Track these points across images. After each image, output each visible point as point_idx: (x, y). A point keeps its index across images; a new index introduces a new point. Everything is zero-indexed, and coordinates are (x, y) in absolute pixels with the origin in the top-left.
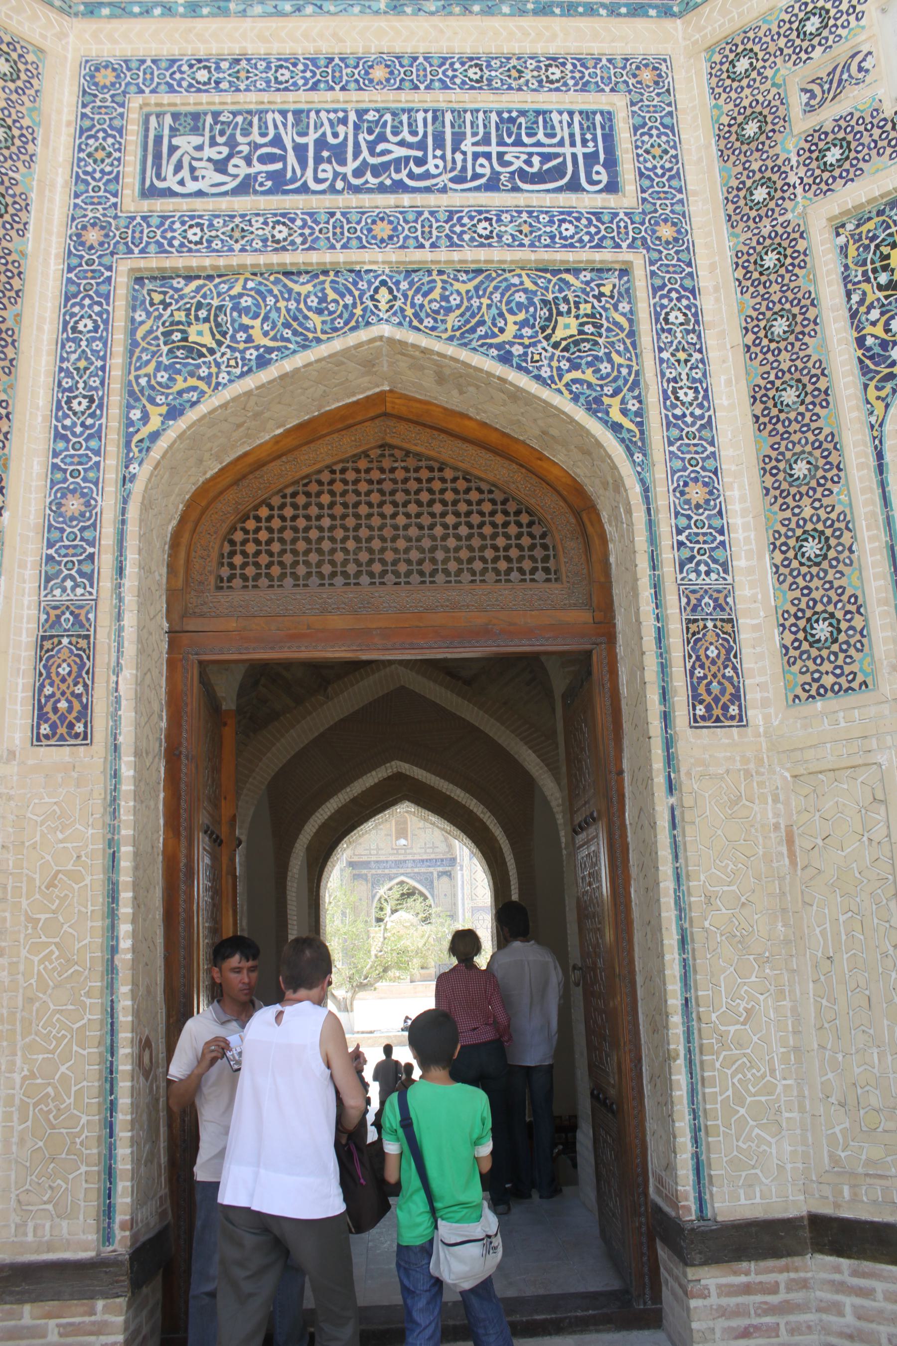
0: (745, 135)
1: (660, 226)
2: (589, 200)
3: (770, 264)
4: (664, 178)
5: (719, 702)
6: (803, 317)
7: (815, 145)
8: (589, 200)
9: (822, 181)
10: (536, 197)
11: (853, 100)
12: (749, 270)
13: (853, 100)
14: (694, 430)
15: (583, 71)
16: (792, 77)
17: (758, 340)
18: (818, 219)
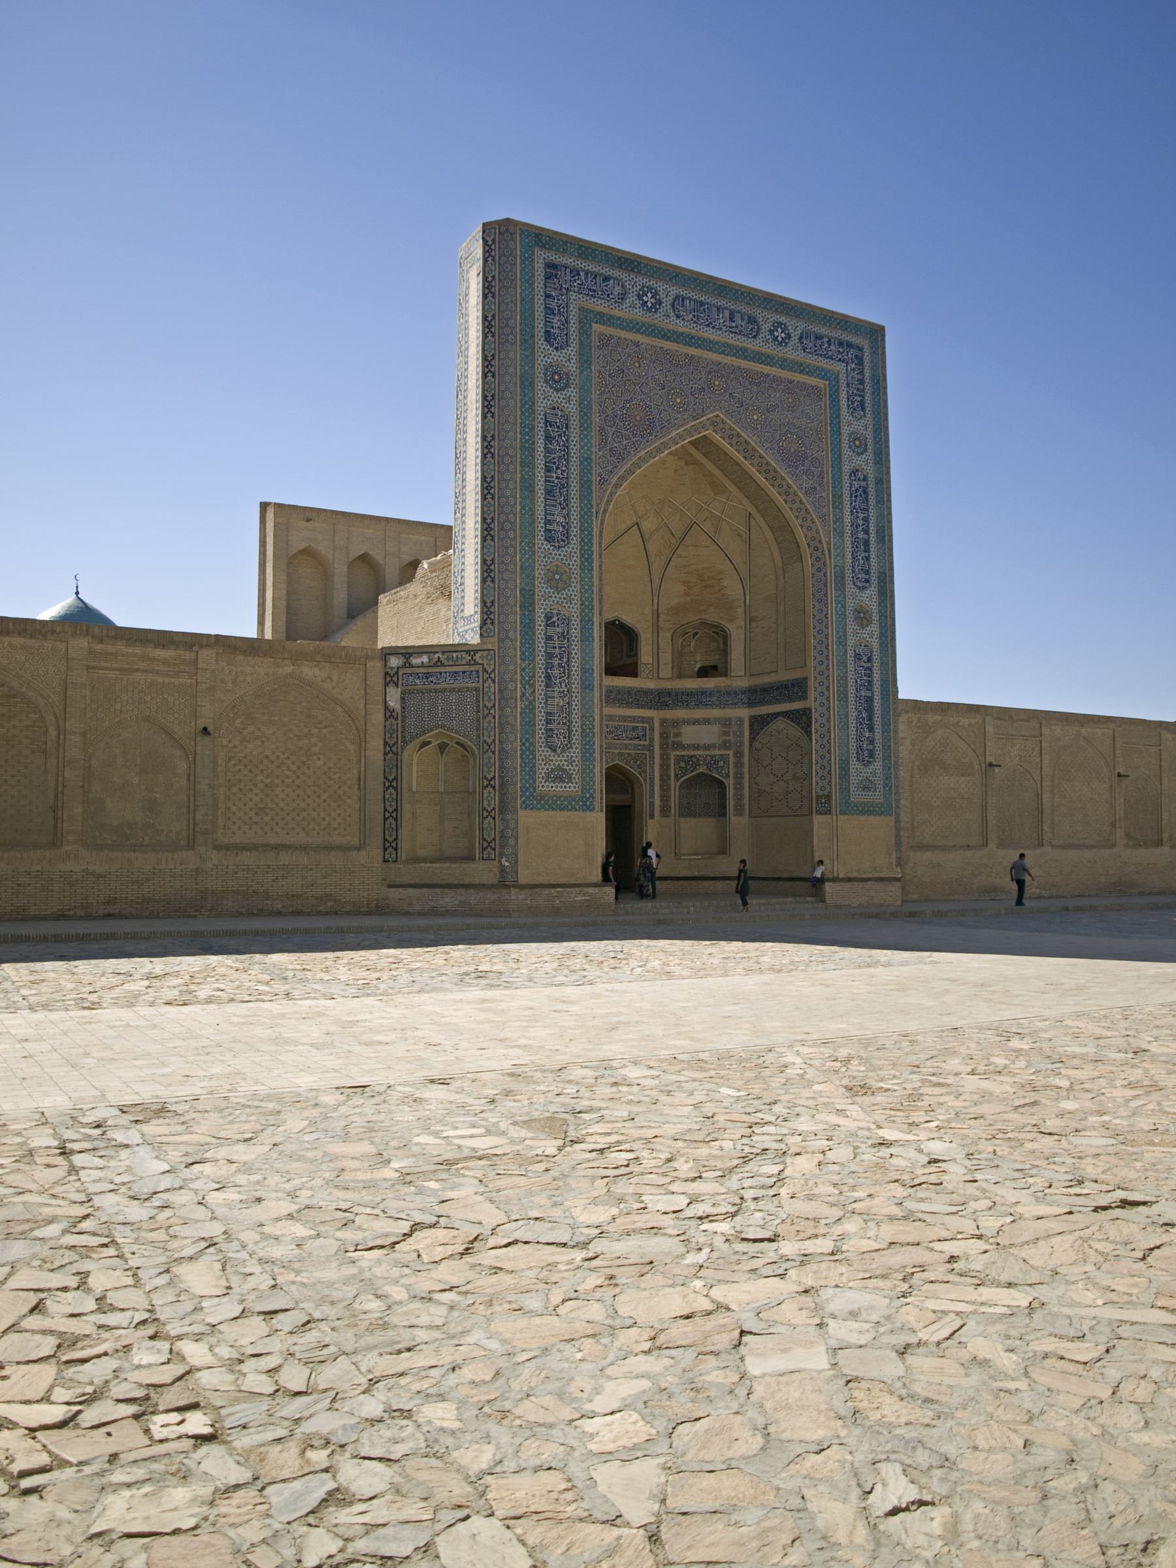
0: (664, 736)
1: (650, 748)
2: (642, 743)
3: (665, 758)
4: (652, 740)
5: (652, 816)
6: (668, 768)
7: (674, 743)
8: (642, 743)
9: (675, 749)
10: (636, 742)
11: (679, 739)
12: (662, 756)
13: (679, 739)
14: (652, 779)
15: (644, 720)
16: (673, 731)
17: (662, 766)
18: (673, 754)
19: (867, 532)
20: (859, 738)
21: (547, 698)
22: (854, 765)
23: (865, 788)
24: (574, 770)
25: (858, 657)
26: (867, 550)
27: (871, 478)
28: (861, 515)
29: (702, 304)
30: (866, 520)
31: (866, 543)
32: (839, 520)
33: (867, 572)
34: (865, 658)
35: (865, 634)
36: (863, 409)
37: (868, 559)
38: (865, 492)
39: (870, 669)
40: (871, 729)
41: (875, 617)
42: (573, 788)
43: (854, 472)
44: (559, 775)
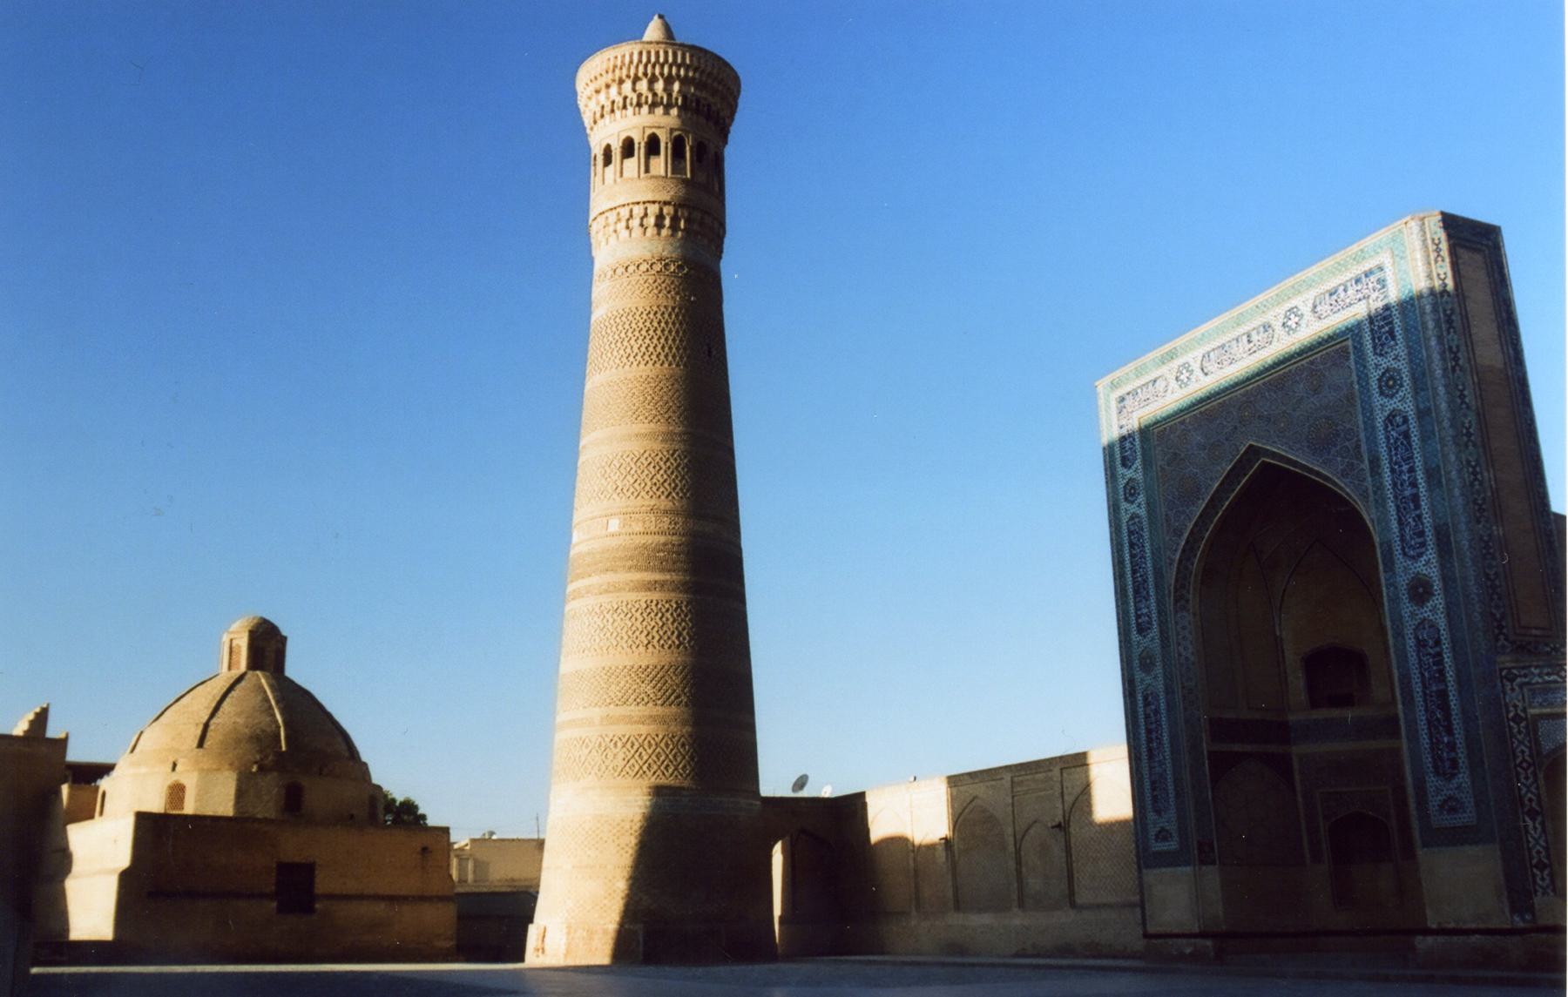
19: (1414, 485)
20: (1435, 745)
21: (1151, 768)
22: (1432, 781)
23: (1453, 810)
24: (1172, 828)
25: (1421, 644)
26: (1418, 507)
27: (1411, 415)
28: (1405, 468)
29: (1223, 346)
30: (1412, 470)
31: (1415, 498)
32: (1379, 487)
33: (1421, 534)
34: (1431, 643)
35: (1426, 612)
36: (1393, 338)
37: (1419, 517)
38: (1406, 435)
39: (1440, 654)
40: (1450, 731)
41: (1437, 585)
42: (1173, 845)
43: (1390, 419)
44: (1163, 835)
